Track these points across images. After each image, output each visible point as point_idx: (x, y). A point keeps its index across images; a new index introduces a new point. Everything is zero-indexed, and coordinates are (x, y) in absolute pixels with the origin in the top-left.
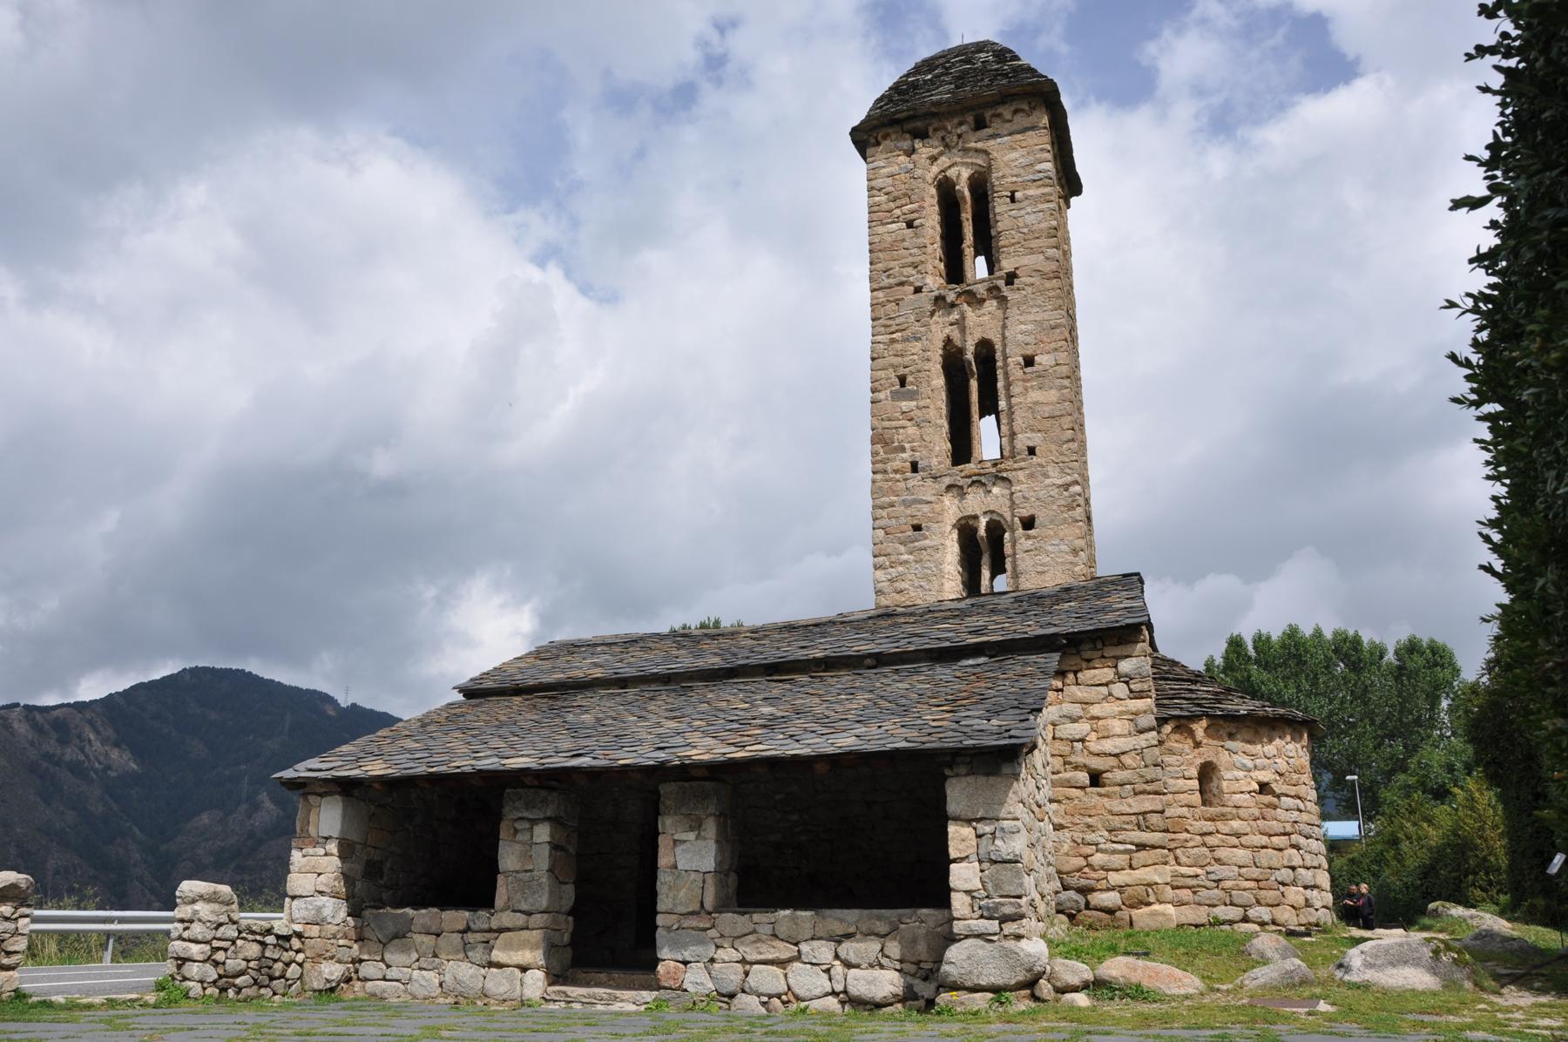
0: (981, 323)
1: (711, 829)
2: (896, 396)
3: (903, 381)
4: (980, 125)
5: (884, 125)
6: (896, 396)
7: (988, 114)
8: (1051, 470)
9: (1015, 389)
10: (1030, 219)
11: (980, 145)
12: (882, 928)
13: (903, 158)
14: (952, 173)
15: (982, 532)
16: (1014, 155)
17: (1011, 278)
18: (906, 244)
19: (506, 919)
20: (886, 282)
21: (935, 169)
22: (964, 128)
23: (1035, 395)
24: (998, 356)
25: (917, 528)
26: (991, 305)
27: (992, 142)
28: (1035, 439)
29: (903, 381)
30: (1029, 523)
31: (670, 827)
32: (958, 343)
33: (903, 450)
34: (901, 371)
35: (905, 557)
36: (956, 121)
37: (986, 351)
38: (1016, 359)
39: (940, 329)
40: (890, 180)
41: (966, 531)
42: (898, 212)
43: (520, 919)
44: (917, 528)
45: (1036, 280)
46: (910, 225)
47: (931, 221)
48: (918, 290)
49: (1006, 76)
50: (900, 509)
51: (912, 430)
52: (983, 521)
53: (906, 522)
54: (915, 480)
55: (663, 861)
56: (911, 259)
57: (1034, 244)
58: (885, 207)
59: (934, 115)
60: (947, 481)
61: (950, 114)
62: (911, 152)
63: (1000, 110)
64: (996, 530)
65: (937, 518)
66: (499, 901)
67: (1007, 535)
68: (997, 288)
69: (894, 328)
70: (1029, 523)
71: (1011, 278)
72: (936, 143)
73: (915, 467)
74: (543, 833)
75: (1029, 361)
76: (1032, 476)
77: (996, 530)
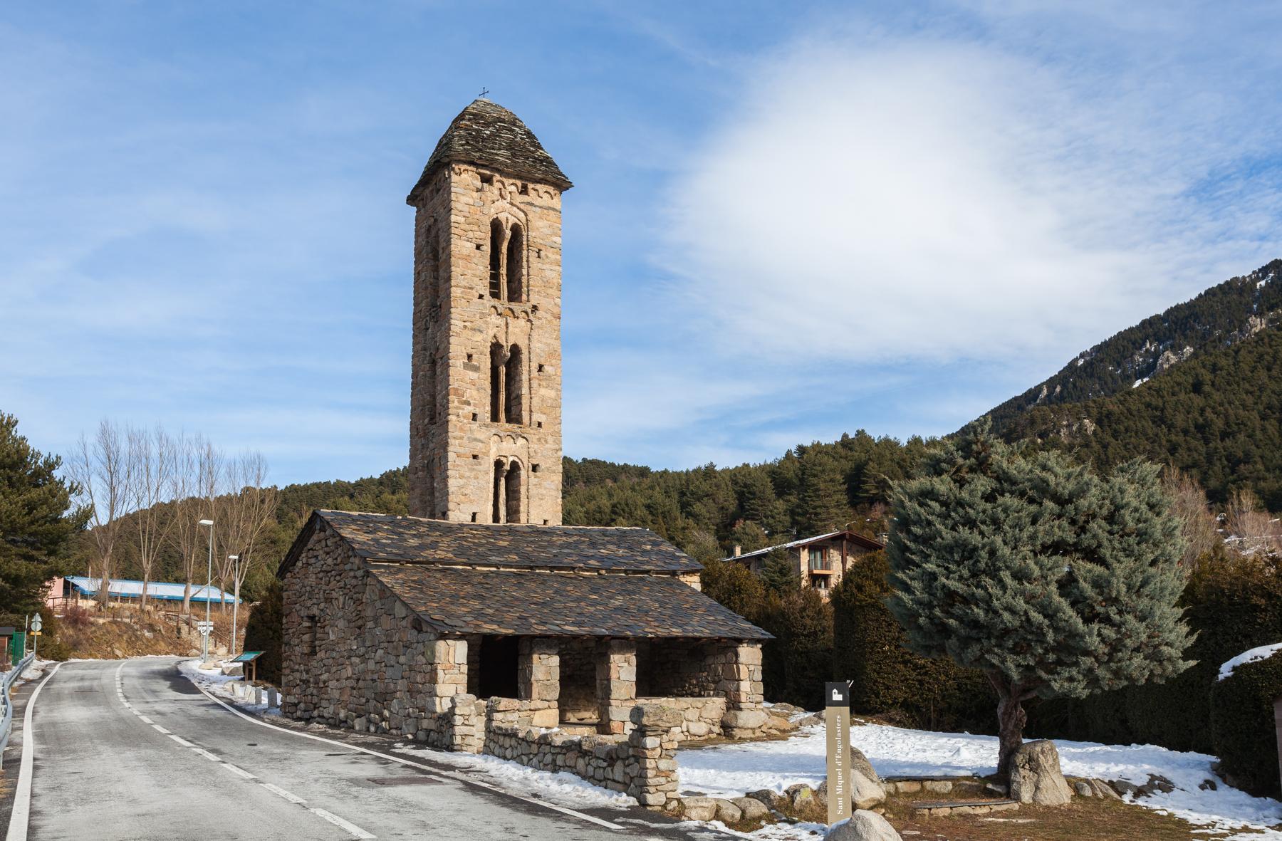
0: (516, 332)
1: (633, 659)
2: (466, 366)
3: (470, 356)
4: (524, 191)
5: (464, 163)
6: (466, 366)
7: (530, 186)
8: (550, 439)
9: (535, 384)
10: (548, 273)
11: (522, 206)
12: (700, 705)
13: (475, 195)
14: (502, 217)
15: (507, 467)
16: (540, 224)
17: (535, 308)
18: (475, 260)
19: (539, 704)
20: (464, 283)
21: (493, 211)
22: (513, 188)
23: (543, 391)
24: (524, 356)
25: (475, 457)
26: (522, 322)
27: (529, 207)
28: (542, 419)
29: (470, 356)
30: (535, 468)
31: (616, 659)
32: (502, 341)
33: (469, 404)
34: (470, 351)
35: (468, 474)
36: (511, 181)
37: (515, 350)
38: (535, 366)
39: (493, 327)
40: (466, 208)
41: (498, 464)
42: (470, 234)
43: (546, 704)
44: (475, 457)
45: (549, 317)
46: (478, 247)
47: (487, 248)
48: (481, 297)
49: (541, 161)
50: (465, 441)
51: (475, 393)
52: (511, 459)
53: (469, 452)
54: (475, 426)
55: (614, 675)
56: (478, 273)
57: (550, 291)
58: (463, 227)
59: (498, 171)
60: (494, 431)
61: (508, 175)
62: (478, 190)
63: (538, 186)
64: (515, 466)
65: (487, 454)
66: (535, 695)
67: (523, 473)
68: (526, 312)
69: (466, 318)
70: (535, 468)
71: (535, 308)
72: (497, 192)
73: (475, 416)
74: (555, 660)
75: (541, 368)
76: (539, 440)
77: (515, 466)
